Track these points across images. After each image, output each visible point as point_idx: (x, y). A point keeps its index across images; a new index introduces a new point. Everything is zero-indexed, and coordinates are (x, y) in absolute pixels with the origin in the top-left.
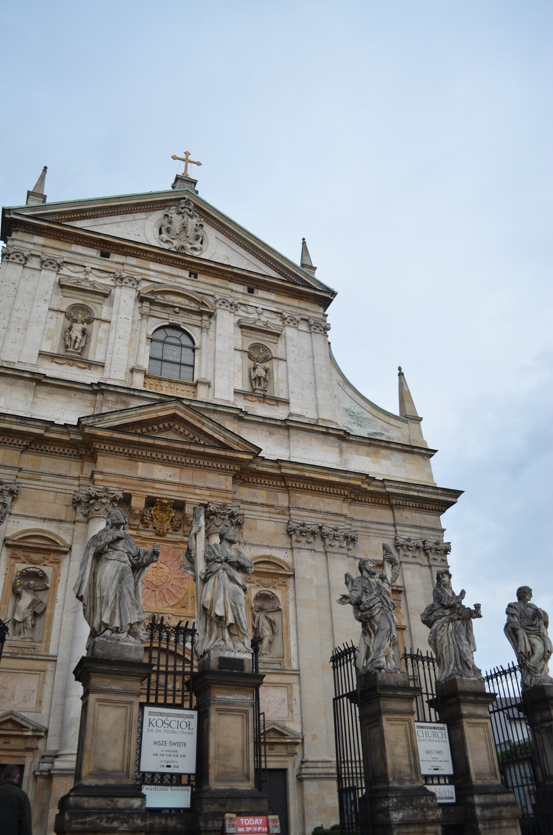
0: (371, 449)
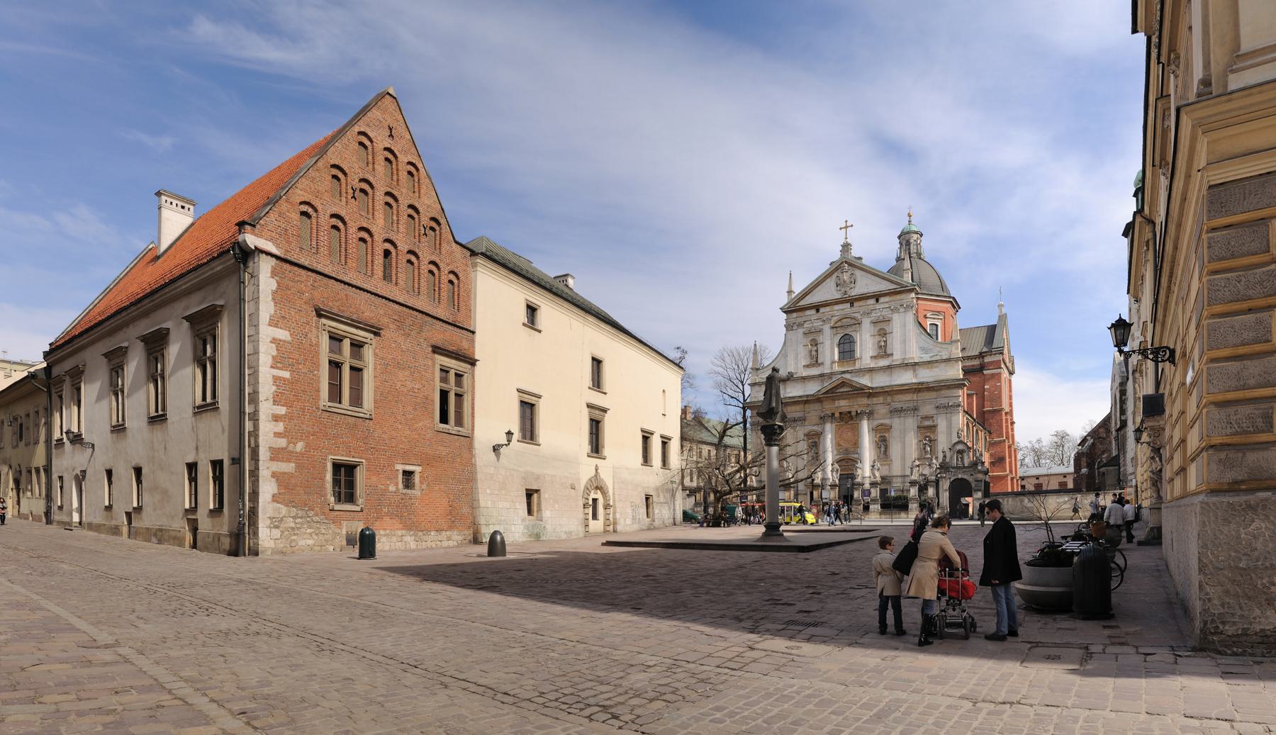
0: (930, 365)
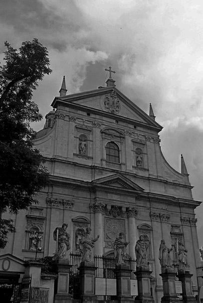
0: (173, 186)
